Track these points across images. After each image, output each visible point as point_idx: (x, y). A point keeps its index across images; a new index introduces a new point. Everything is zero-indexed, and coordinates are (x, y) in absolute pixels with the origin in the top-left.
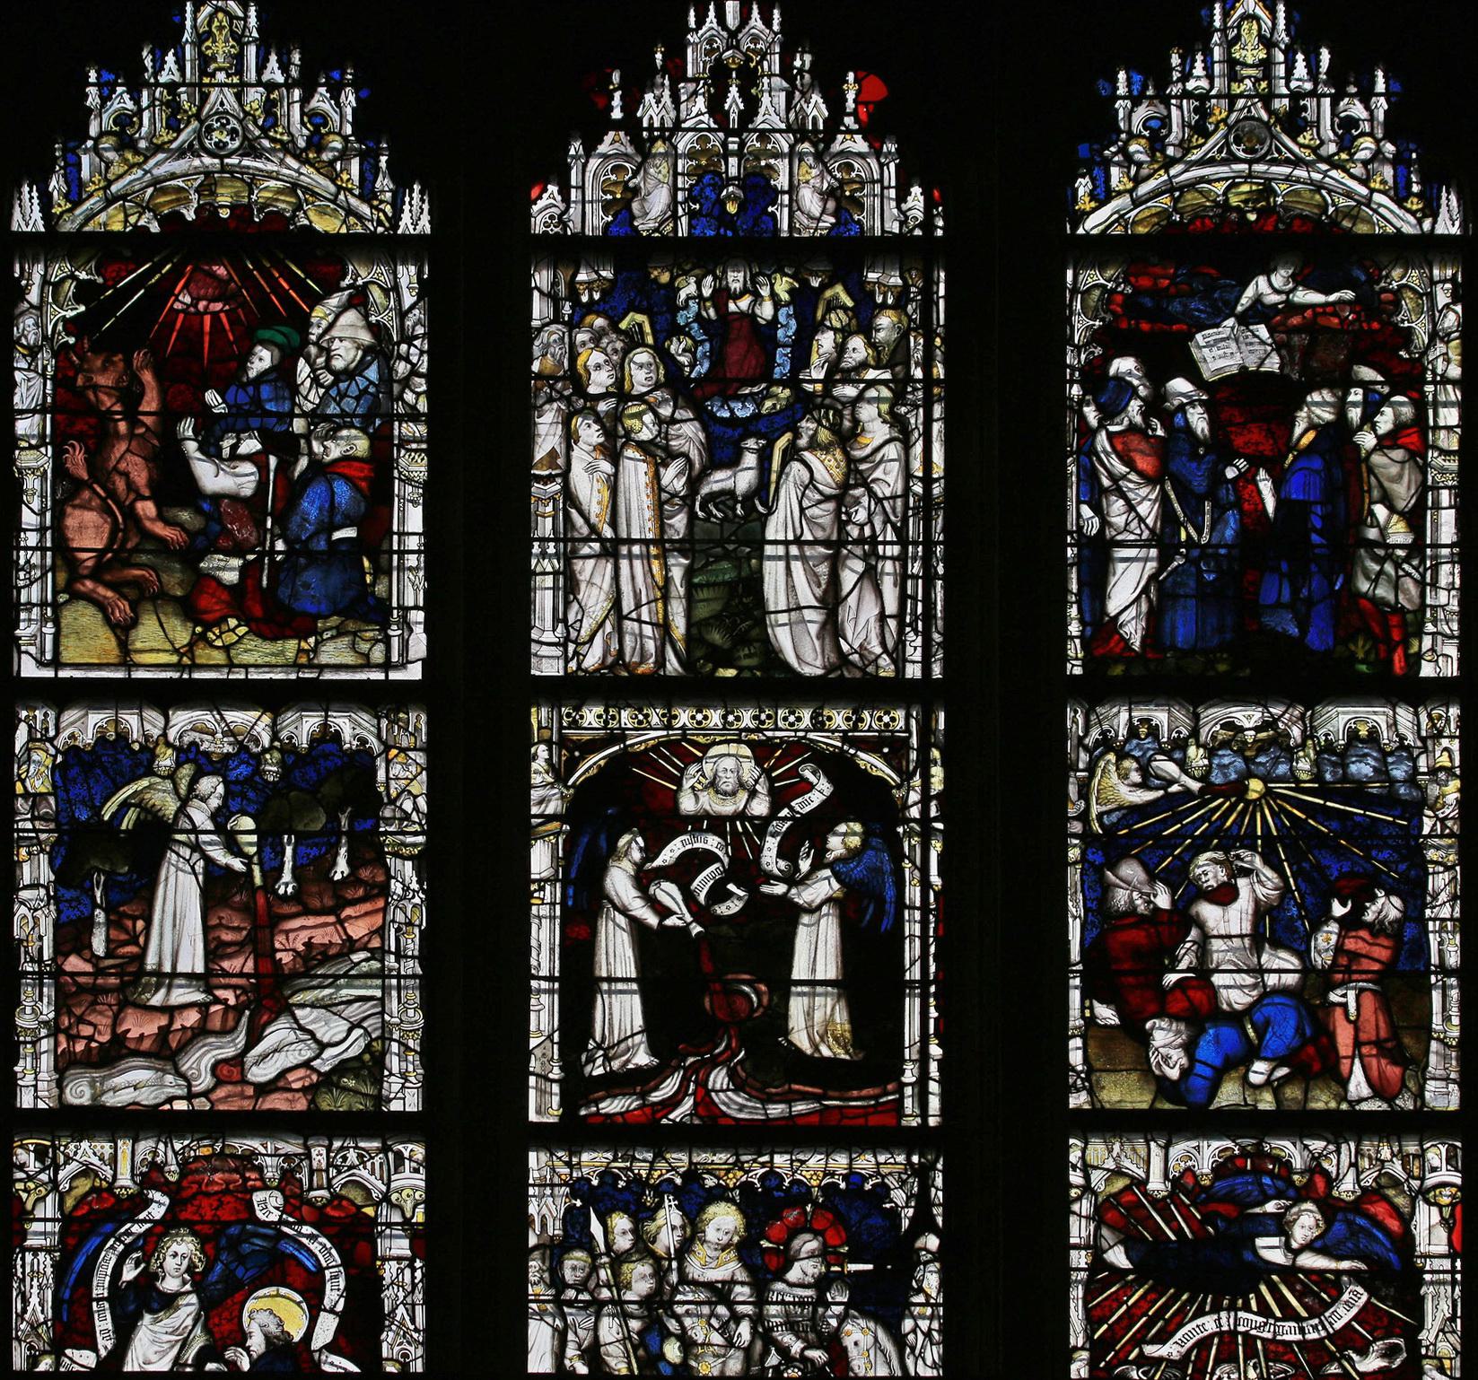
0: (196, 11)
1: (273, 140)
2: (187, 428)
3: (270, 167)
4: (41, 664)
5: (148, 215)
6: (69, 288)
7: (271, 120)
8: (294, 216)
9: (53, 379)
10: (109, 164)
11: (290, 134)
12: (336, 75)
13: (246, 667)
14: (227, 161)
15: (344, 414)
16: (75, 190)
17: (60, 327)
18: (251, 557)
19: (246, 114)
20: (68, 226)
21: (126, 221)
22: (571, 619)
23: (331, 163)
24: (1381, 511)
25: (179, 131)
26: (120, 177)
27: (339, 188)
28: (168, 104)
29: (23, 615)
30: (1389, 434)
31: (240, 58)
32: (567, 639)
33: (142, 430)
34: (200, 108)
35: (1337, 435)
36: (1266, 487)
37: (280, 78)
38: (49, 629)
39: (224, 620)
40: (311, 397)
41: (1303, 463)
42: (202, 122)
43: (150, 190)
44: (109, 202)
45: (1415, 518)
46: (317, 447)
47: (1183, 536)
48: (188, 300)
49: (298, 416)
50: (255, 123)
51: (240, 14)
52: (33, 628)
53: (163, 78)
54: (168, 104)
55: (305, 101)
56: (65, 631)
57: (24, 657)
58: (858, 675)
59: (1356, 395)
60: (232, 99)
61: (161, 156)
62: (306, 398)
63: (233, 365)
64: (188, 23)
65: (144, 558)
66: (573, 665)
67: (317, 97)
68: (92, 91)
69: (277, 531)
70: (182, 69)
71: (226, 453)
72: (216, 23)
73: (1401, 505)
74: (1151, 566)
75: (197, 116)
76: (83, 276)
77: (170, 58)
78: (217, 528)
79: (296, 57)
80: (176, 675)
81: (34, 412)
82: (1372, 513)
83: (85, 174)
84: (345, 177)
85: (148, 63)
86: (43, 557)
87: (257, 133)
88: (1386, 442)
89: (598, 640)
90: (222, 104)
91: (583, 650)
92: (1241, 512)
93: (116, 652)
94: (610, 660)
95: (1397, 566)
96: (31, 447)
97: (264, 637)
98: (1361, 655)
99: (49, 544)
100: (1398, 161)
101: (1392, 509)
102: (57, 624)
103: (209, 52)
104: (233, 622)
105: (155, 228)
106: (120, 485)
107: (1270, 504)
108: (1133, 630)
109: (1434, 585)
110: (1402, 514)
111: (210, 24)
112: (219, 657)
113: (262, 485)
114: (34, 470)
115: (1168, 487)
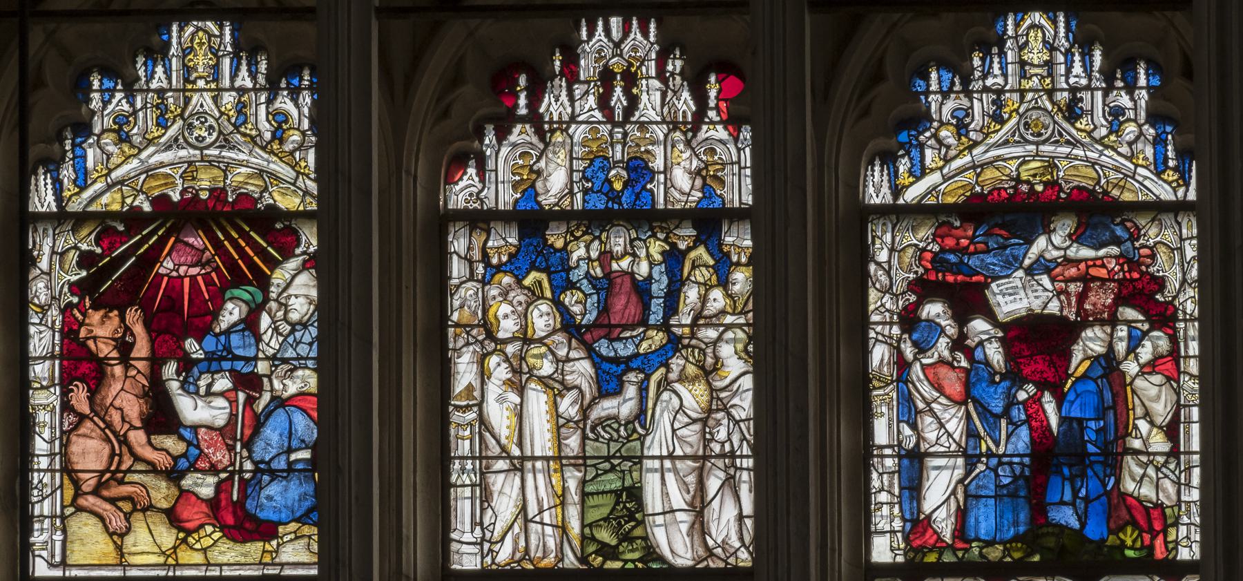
0: (181, 30)
1: (244, 135)
2: (170, 370)
3: (242, 157)
4: (52, 565)
5: (142, 197)
6: (73, 257)
7: (242, 118)
8: (261, 197)
9: (61, 331)
10: (109, 156)
11: (257, 129)
12: (296, 82)
13: (220, 565)
14: (206, 152)
15: (299, 358)
16: (81, 176)
17: (66, 289)
18: (223, 475)
19: (222, 114)
20: (75, 206)
21: (123, 202)
22: (486, 523)
23: (292, 153)
24: (1143, 426)
25: (166, 128)
26: (119, 166)
27: (298, 173)
28: (157, 107)
29: (37, 526)
30: (1148, 364)
31: (216, 68)
32: (483, 539)
33: (134, 373)
34: (183, 110)
35: (1108, 364)
36: (1050, 407)
37: (249, 84)
38: (58, 537)
39: (202, 526)
40: (272, 344)
41: (1080, 388)
42: (184, 120)
43: (143, 177)
44: (109, 187)
45: (1171, 431)
46: (277, 384)
47: (984, 448)
48: (171, 265)
49: (262, 359)
50: (229, 120)
51: (217, 33)
52: (45, 536)
53: (154, 85)
54: (157, 107)
55: (269, 102)
56: (70, 538)
57: (37, 559)
58: (722, 565)
59: (1122, 331)
60: (210, 101)
61: (151, 149)
62: (268, 345)
63: (209, 318)
64: (174, 41)
65: (136, 477)
66: (488, 560)
67: (280, 99)
68: (96, 96)
69: (245, 453)
70: (169, 78)
71: (202, 391)
72: (197, 41)
73: (1159, 420)
74: (959, 473)
75: (181, 115)
76: (84, 247)
77: (159, 70)
78: (197, 452)
79: (263, 67)
80: (162, 573)
81: (44, 358)
82: (1136, 427)
83: (90, 164)
84: (303, 164)
85: (141, 73)
86: (53, 478)
87: (231, 128)
88: (1150, 368)
89: (509, 539)
90: (202, 106)
91: (496, 548)
92: (1031, 428)
93: (114, 554)
94: (518, 556)
95: (1158, 469)
96: (42, 388)
97: (234, 539)
98: (1129, 542)
99: (58, 467)
100: (1158, 142)
101: (1152, 423)
102: (64, 531)
103: (191, 64)
104: (209, 529)
105: (147, 207)
106: (116, 417)
107: (1054, 421)
108: (944, 524)
109: (1188, 485)
110: (1160, 427)
111: (192, 41)
112: (198, 558)
113: (233, 416)
114: (45, 407)
115: (971, 407)
